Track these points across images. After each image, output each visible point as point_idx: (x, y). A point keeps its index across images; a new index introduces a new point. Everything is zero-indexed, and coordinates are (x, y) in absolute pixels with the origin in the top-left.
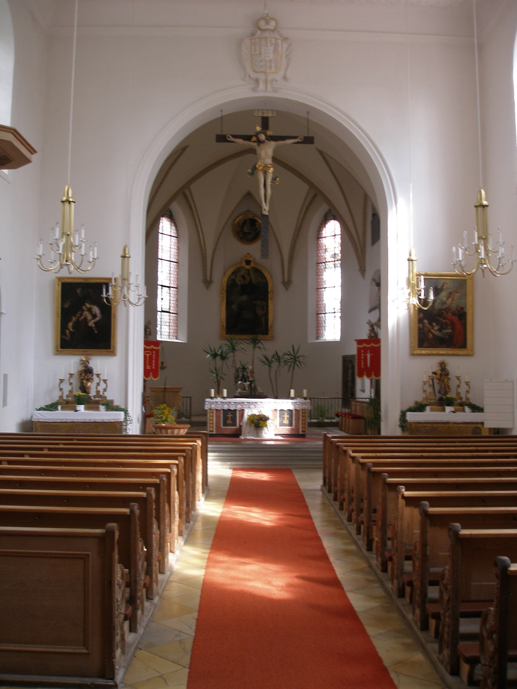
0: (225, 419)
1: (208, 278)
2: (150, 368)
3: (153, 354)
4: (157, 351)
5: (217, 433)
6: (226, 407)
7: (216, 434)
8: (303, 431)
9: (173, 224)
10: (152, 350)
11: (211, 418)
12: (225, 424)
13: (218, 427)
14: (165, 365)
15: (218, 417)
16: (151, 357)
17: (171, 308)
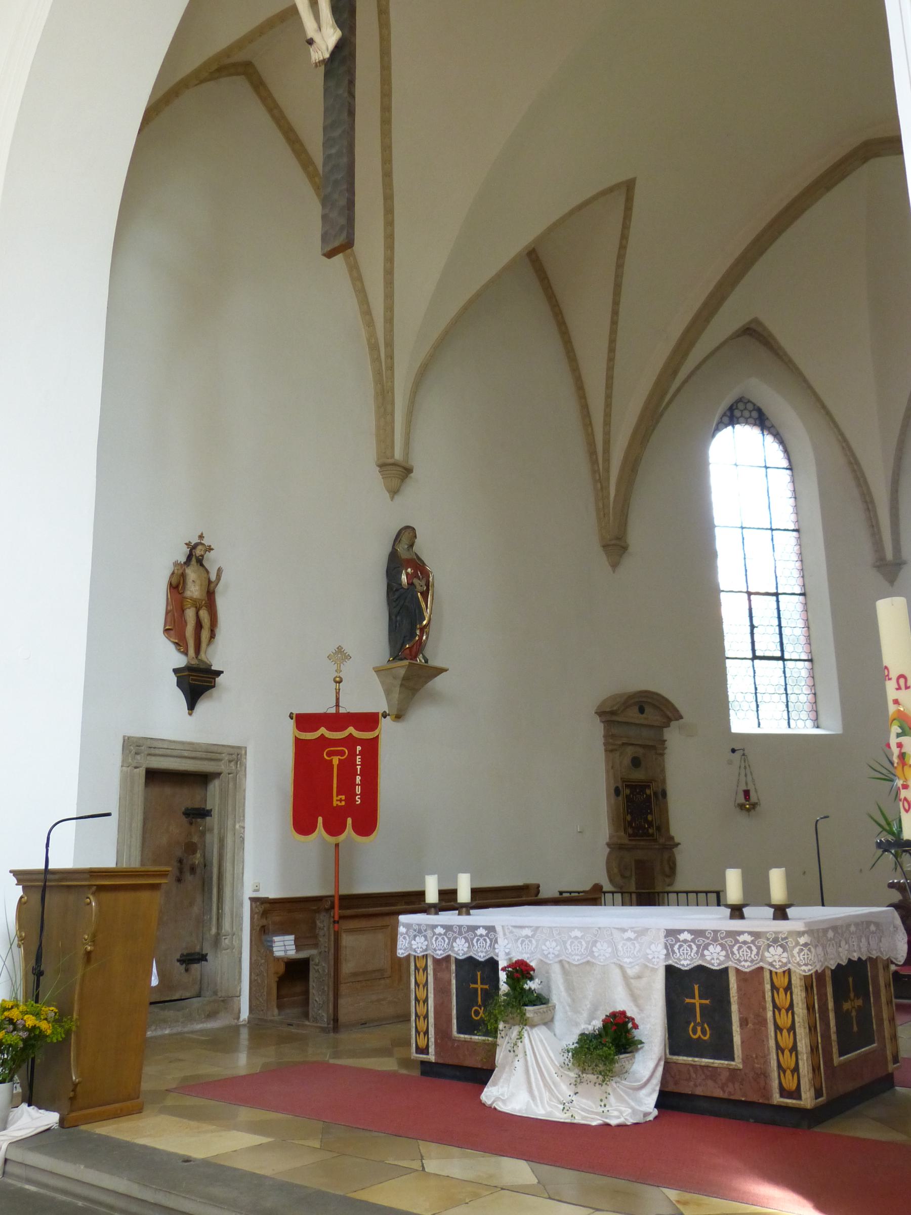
0: (466, 999)
1: (889, 555)
2: (343, 803)
3: (353, 754)
4: (372, 748)
5: (441, 1061)
6: (460, 949)
7: (436, 1063)
8: (784, 1092)
9: (769, 439)
10: (350, 741)
11: (421, 994)
12: (467, 1026)
13: (443, 1034)
14: (753, 797)
15: (442, 990)
16: (347, 768)
17: (788, 648)
